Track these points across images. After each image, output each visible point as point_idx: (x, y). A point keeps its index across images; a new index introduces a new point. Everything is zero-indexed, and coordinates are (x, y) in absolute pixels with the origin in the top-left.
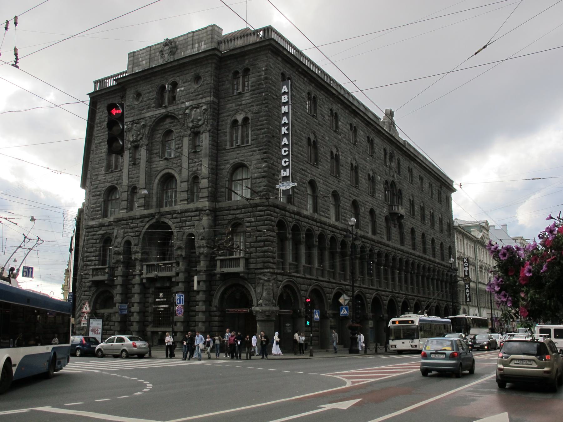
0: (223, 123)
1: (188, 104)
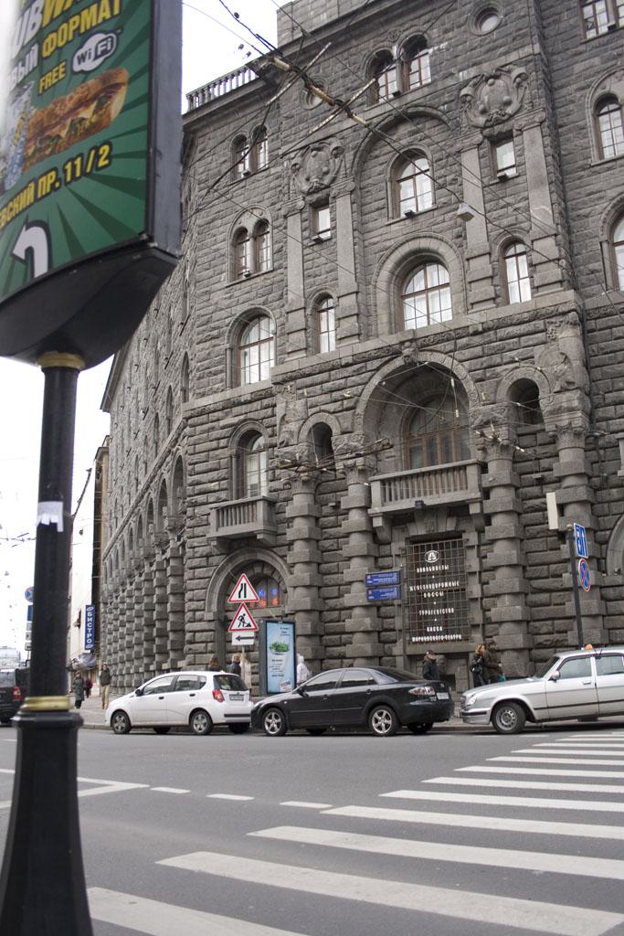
0: (571, 107)
1: (463, 76)
